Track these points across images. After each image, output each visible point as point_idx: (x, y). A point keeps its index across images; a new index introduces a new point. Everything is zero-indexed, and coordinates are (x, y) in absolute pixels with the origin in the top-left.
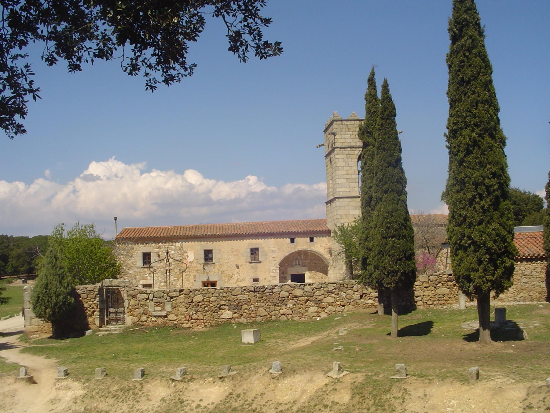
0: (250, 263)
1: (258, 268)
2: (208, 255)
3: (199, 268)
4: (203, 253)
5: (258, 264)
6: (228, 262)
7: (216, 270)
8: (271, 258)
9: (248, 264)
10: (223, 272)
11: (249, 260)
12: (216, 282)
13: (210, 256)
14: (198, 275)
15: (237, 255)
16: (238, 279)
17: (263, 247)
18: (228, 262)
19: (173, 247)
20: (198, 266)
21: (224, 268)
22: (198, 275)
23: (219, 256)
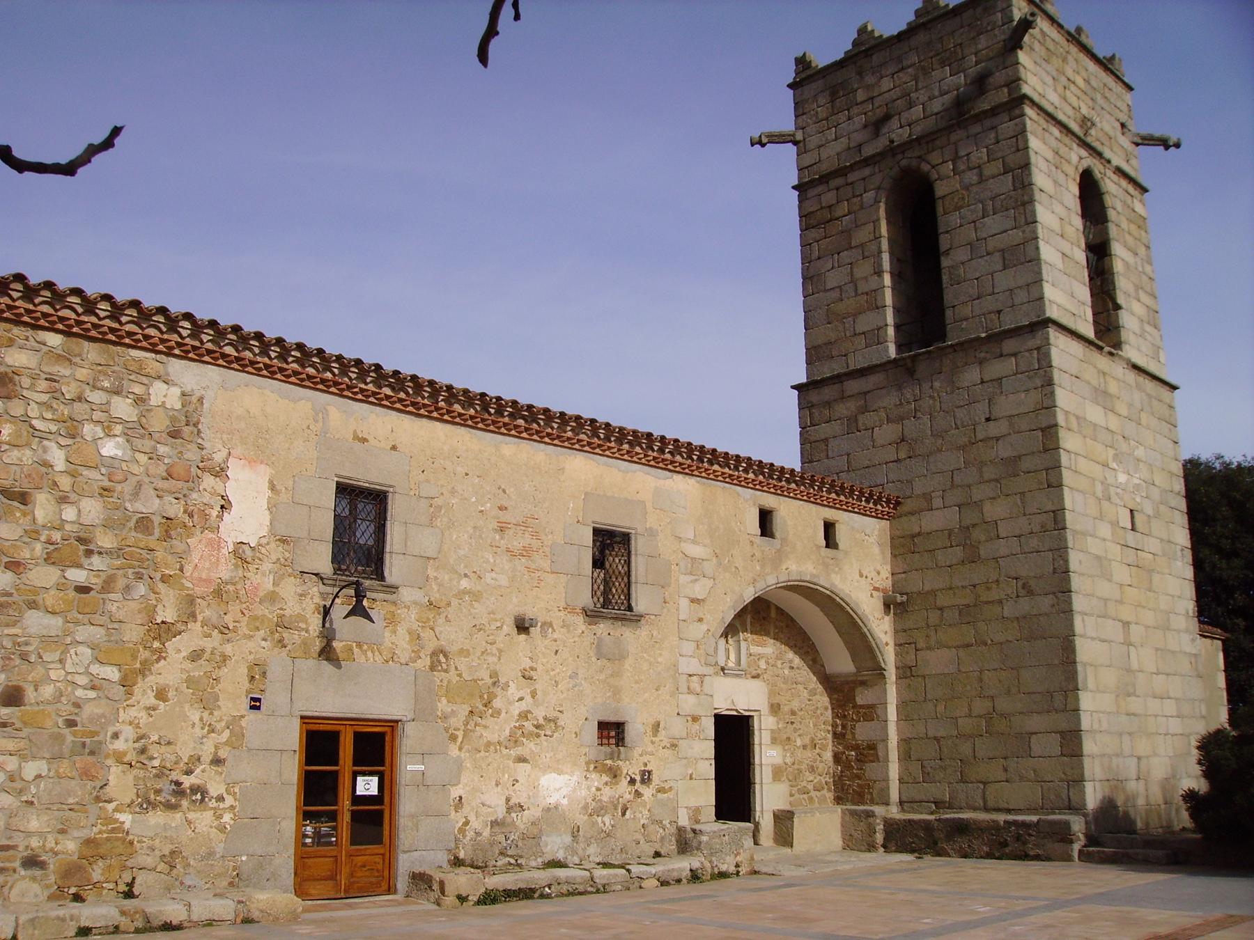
0: (591, 616)
1: (622, 657)
2: (361, 527)
3: (292, 607)
4: (329, 497)
5: (629, 636)
6: (476, 596)
7: (400, 640)
8: (684, 603)
9: (580, 620)
10: (439, 656)
11: (585, 598)
12: (393, 724)
13: (364, 534)
14: (278, 664)
15: (526, 552)
16: (524, 715)
17: (652, 533)
18: (476, 596)
19: (123, 408)
20: (289, 588)
21: (451, 634)
22: (278, 664)
23: (426, 541)
